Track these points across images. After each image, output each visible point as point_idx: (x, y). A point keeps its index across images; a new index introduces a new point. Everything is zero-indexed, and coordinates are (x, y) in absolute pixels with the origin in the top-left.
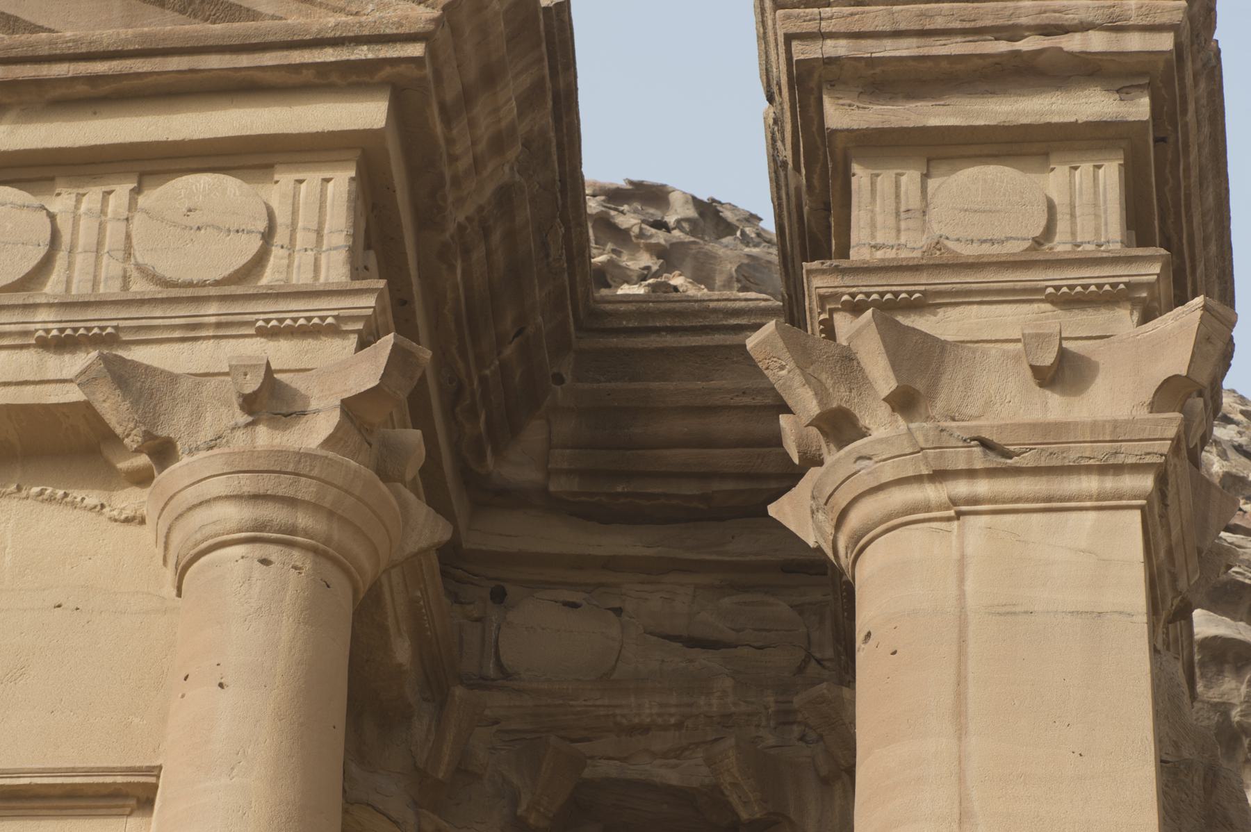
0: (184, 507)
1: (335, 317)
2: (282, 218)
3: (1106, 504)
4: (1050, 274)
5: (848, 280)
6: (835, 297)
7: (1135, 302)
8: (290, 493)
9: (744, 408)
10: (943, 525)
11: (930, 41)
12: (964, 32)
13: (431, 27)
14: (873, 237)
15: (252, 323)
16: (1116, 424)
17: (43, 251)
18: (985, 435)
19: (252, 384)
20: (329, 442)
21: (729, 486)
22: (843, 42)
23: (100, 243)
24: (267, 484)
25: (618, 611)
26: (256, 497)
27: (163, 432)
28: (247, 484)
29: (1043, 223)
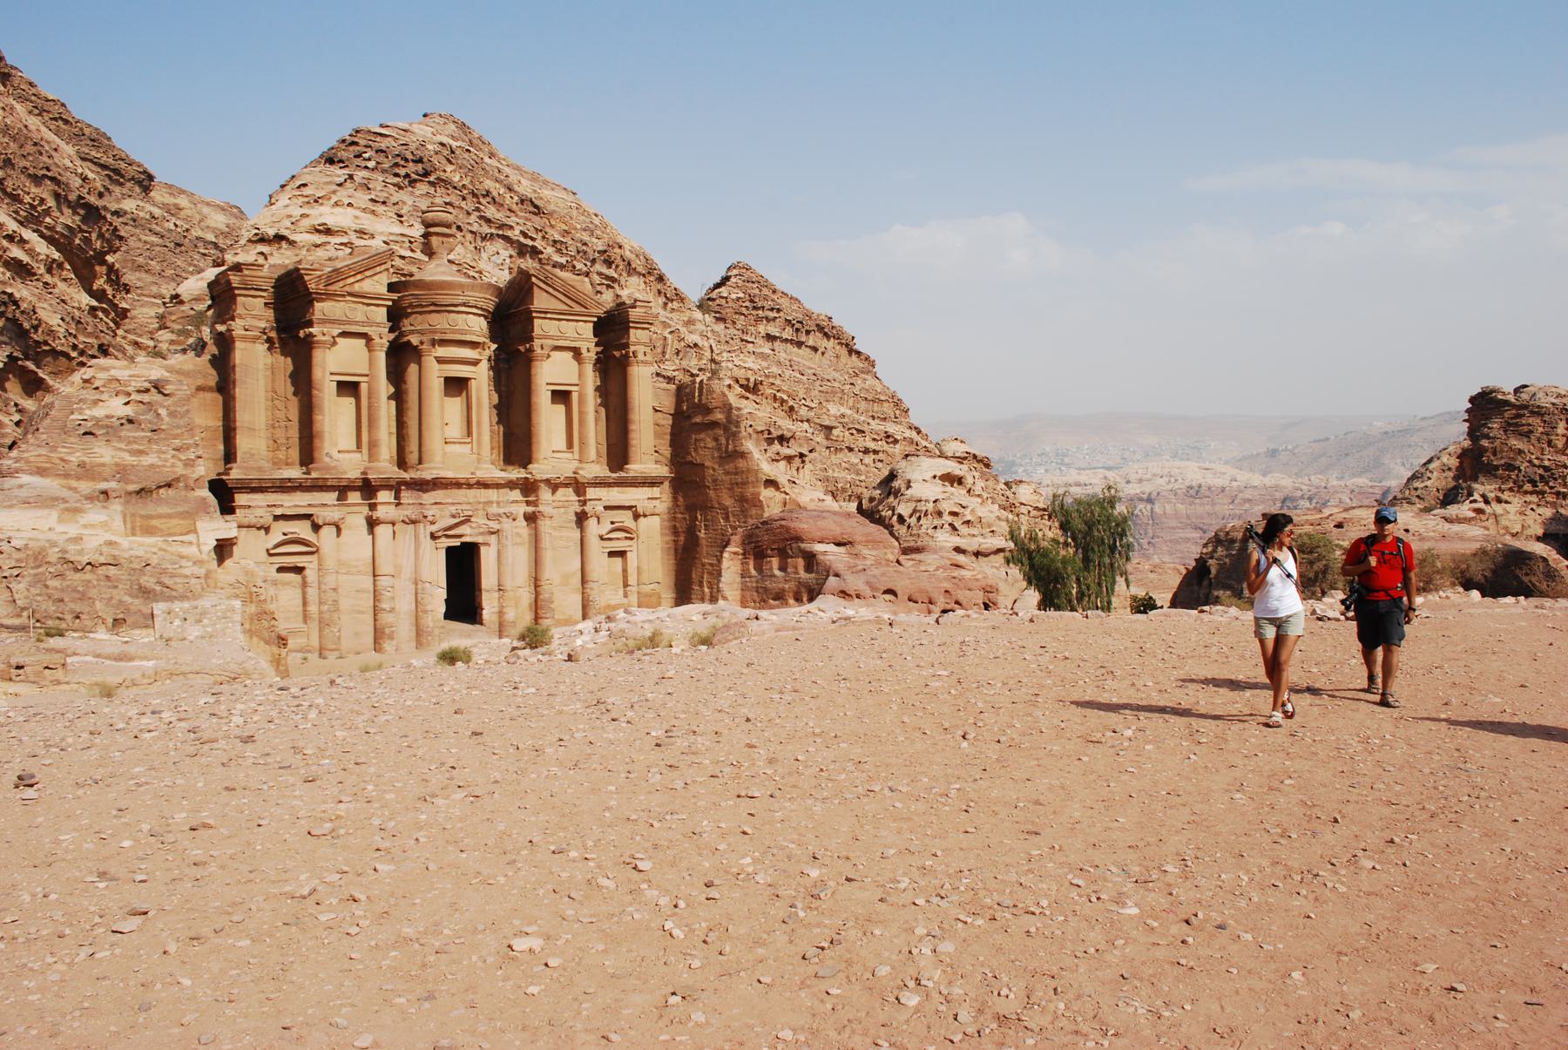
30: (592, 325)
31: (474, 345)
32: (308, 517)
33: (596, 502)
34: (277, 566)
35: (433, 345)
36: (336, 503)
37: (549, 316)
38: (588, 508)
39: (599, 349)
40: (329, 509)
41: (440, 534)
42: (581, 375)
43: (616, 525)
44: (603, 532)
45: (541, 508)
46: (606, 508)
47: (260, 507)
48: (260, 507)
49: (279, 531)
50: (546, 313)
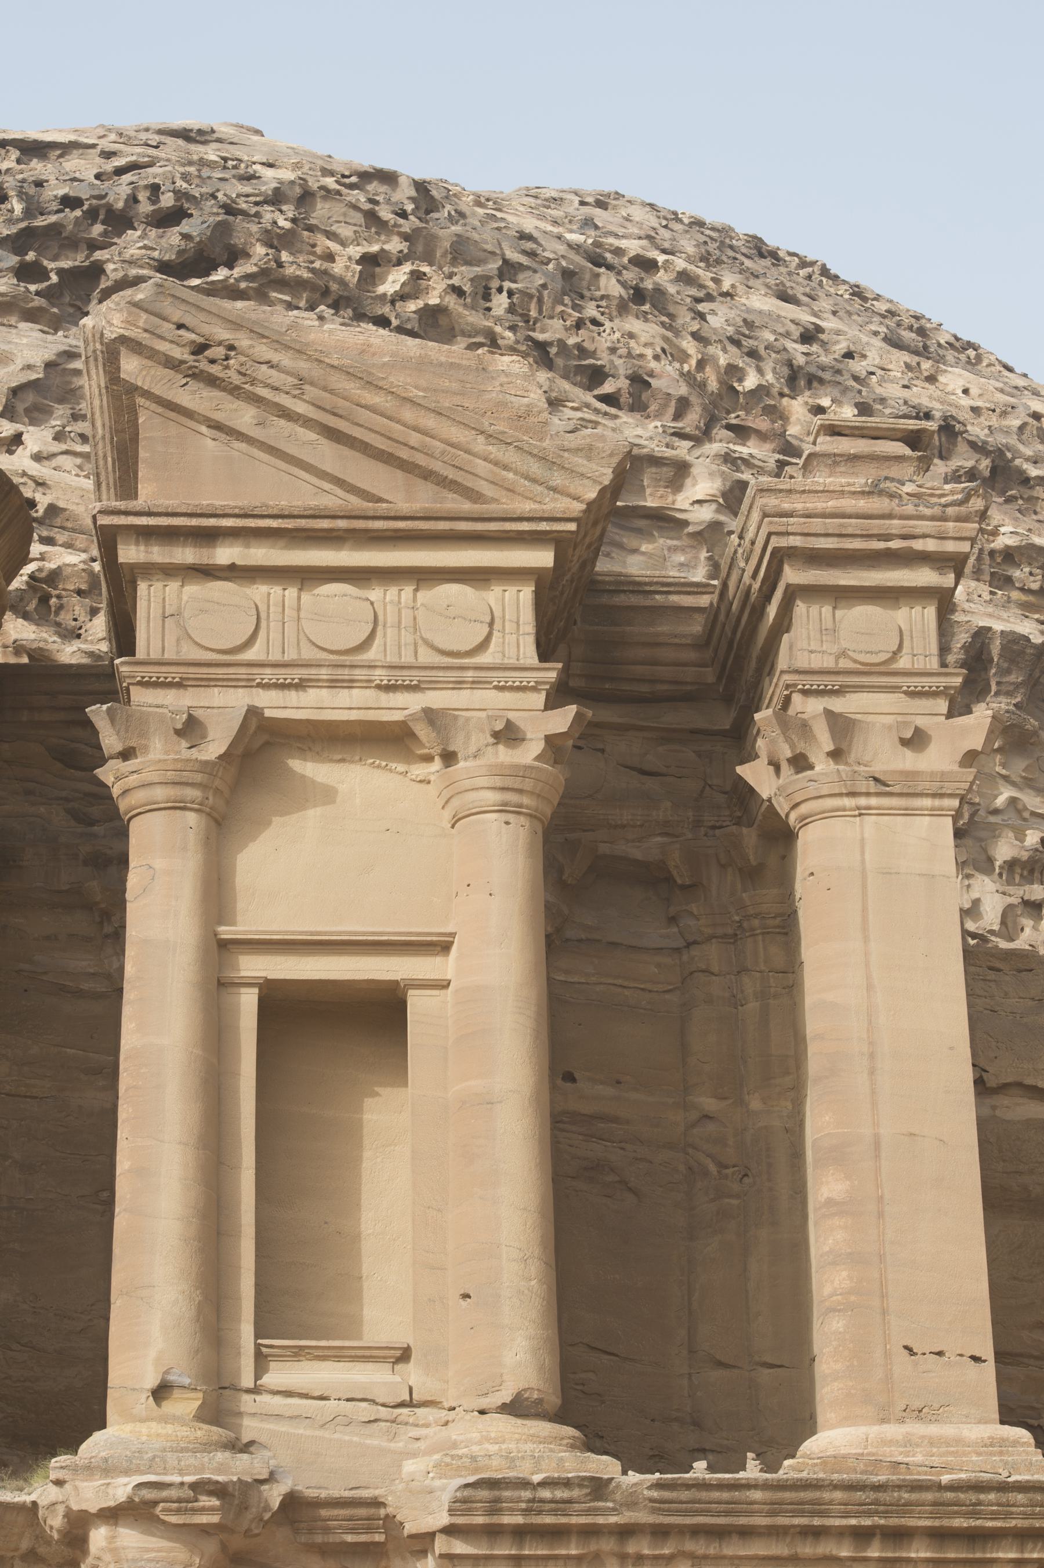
0: (463, 789)
1: (536, 682)
2: (497, 614)
3: (935, 813)
4: (905, 679)
5: (802, 677)
6: (795, 685)
7: (946, 695)
8: (520, 787)
9: (676, 644)
10: (852, 819)
11: (844, 539)
12: (862, 536)
13: (581, 515)
14: (809, 645)
15: (491, 682)
16: (943, 773)
17: (370, 627)
18: (877, 776)
19: (499, 726)
20: (538, 758)
21: (665, 687)
22: (798, 538)
23: (400, 622)
24: (509, 782)
25: (603, 751)
26: (503, 789)
27: (451, 748)
28: (498, 781)
29: (898, 643)
37: (225, 554)
39: (562, 719)
50: (209, 536)
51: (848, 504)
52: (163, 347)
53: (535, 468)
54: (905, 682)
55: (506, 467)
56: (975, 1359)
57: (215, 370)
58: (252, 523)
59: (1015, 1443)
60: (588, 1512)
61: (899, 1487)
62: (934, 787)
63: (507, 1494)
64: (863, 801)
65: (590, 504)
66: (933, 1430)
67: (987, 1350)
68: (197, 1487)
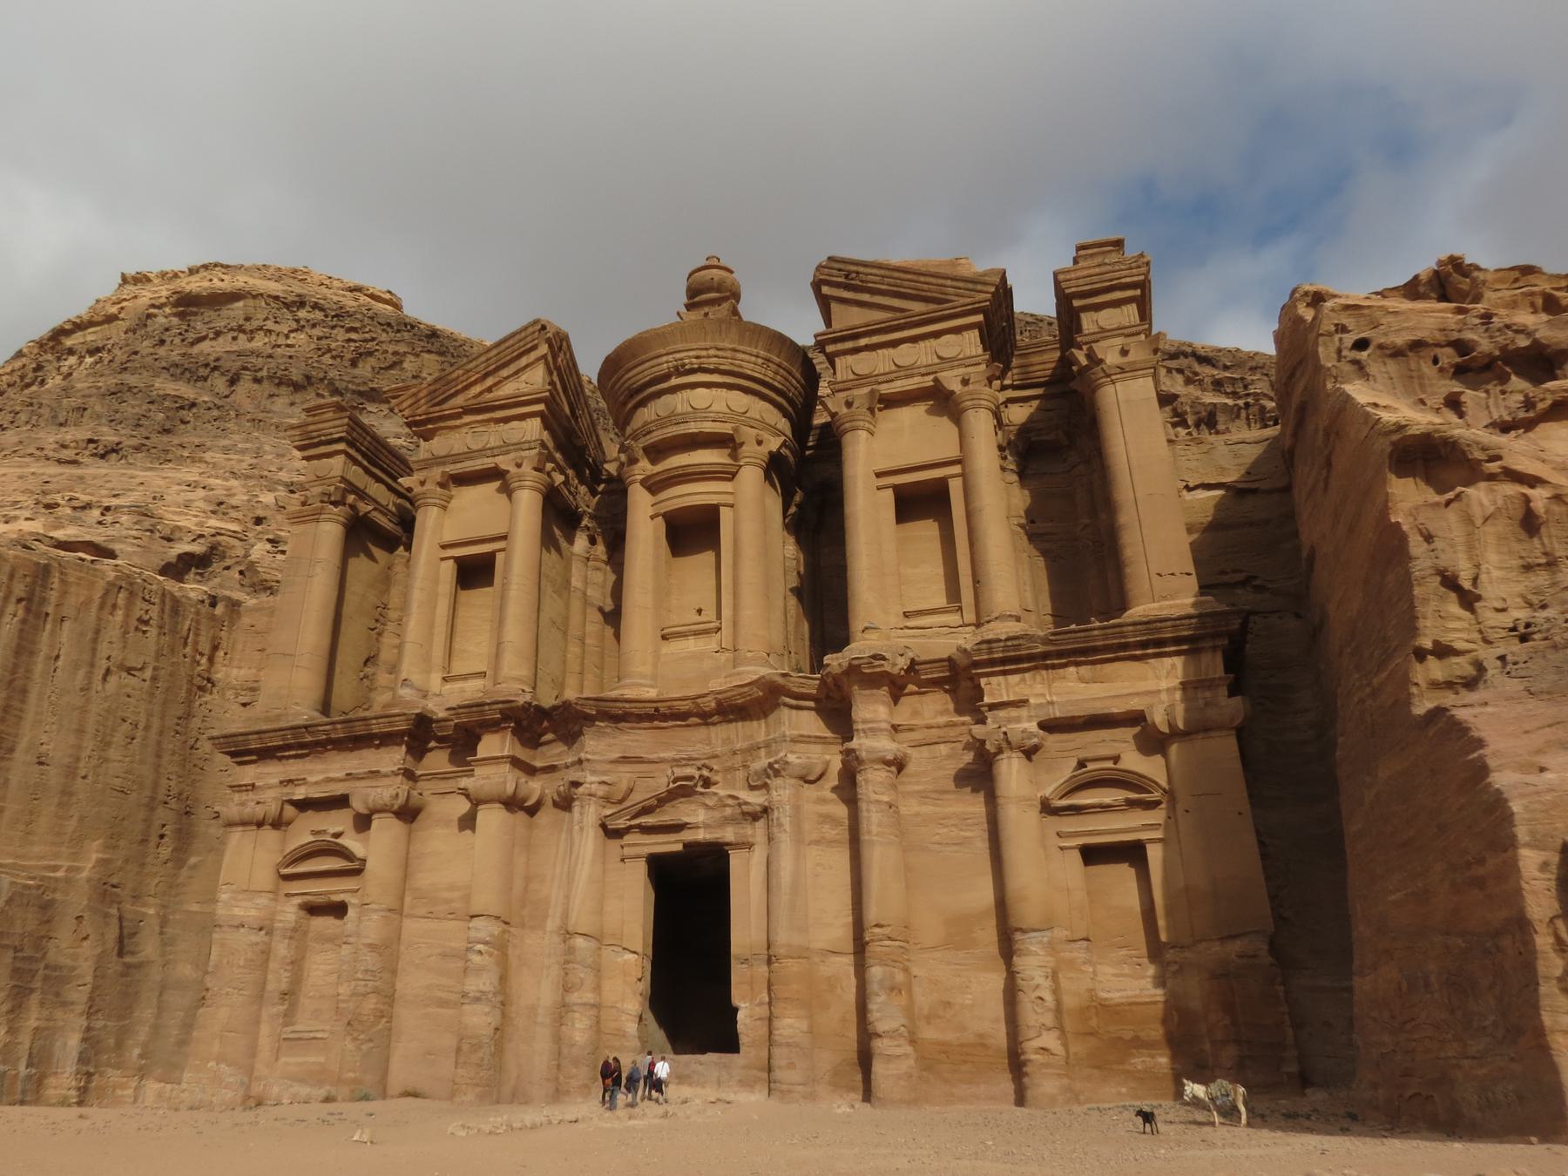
3: (1143, 376)
30: (974, 335)
31: (726, 441)
32: (341, 802)
33: (1013, 712)
34: (298, 900)
35: (633, 461)
36: (395, 769)
37: (863, 342)
38: (988, 731)
40: (386, 781)
41: (621, 823)
42: (962, 437)
43: (1091, 766)
44: (1050, 788)
45: (854, 744)
46: (1049, 726)
47: (270, 787)
48: (270, 787)
49: (304, 832)
51: (1092, 271)
52: (835, 279)
53: (970, 286)
54: (1126, 331)
55: (960, 288)
56: (1189, 574)
57: (853, 282)
58: (870, 328)
59: (1207, 602)
60: (1028, 648)
61: (1155, 622)
62: (1142, 366)
63: (994, 645)
64: (1114, 377)
65: (993, 293)
66: (1171, 602)
67: (1193, 571)
68: (875, 657)
